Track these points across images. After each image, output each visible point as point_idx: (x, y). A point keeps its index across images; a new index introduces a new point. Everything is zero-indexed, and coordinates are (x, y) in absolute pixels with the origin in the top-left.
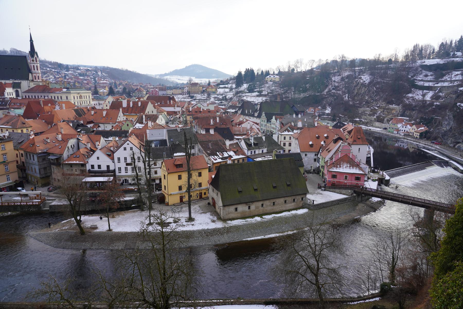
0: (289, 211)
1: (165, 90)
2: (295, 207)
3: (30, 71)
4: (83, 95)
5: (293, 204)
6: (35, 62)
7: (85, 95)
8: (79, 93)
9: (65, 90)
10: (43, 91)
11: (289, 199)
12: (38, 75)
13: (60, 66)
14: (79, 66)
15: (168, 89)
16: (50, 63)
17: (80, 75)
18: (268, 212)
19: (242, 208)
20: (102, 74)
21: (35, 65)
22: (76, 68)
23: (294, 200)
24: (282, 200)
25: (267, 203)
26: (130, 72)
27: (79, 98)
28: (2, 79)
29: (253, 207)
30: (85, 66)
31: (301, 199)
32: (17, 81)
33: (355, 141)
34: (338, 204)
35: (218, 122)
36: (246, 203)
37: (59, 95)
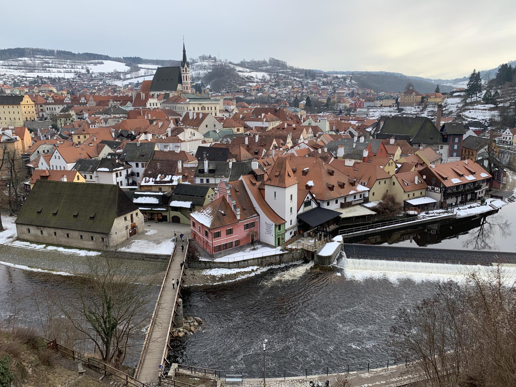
0: (89, 250)
1: (372, 101)
2: (94, 248)
3: (180, 82)
4: (206, 106)
5: (91, 243)
6: (185, 72)
7: (210, 106)
8: (200, 104)
9: (188, 100)
10: (174, 101)
11: (85, 235)
12: (186, 85)
13: (311, 74)
14: (330, 73)
15: (377, 100)
16: (302, 71)
17: (324, 84)
18: (63, 243)
19: (34, 231)
20: (351, 80)
21: (185, 75)
22: (326, 76)
23: (92, 238)
24: (76, 234)
25: (59, 232)
26: (405, 76)
27: (200, 109)
28: (158, 91)
29: (46, 232)
30: (343, 73)
31: (101, 239)
32: (168, 92)
33: (270, 179)
34: (143, 260)
35: (257, 141)
36: (37, 226)
37: (183, 106)
